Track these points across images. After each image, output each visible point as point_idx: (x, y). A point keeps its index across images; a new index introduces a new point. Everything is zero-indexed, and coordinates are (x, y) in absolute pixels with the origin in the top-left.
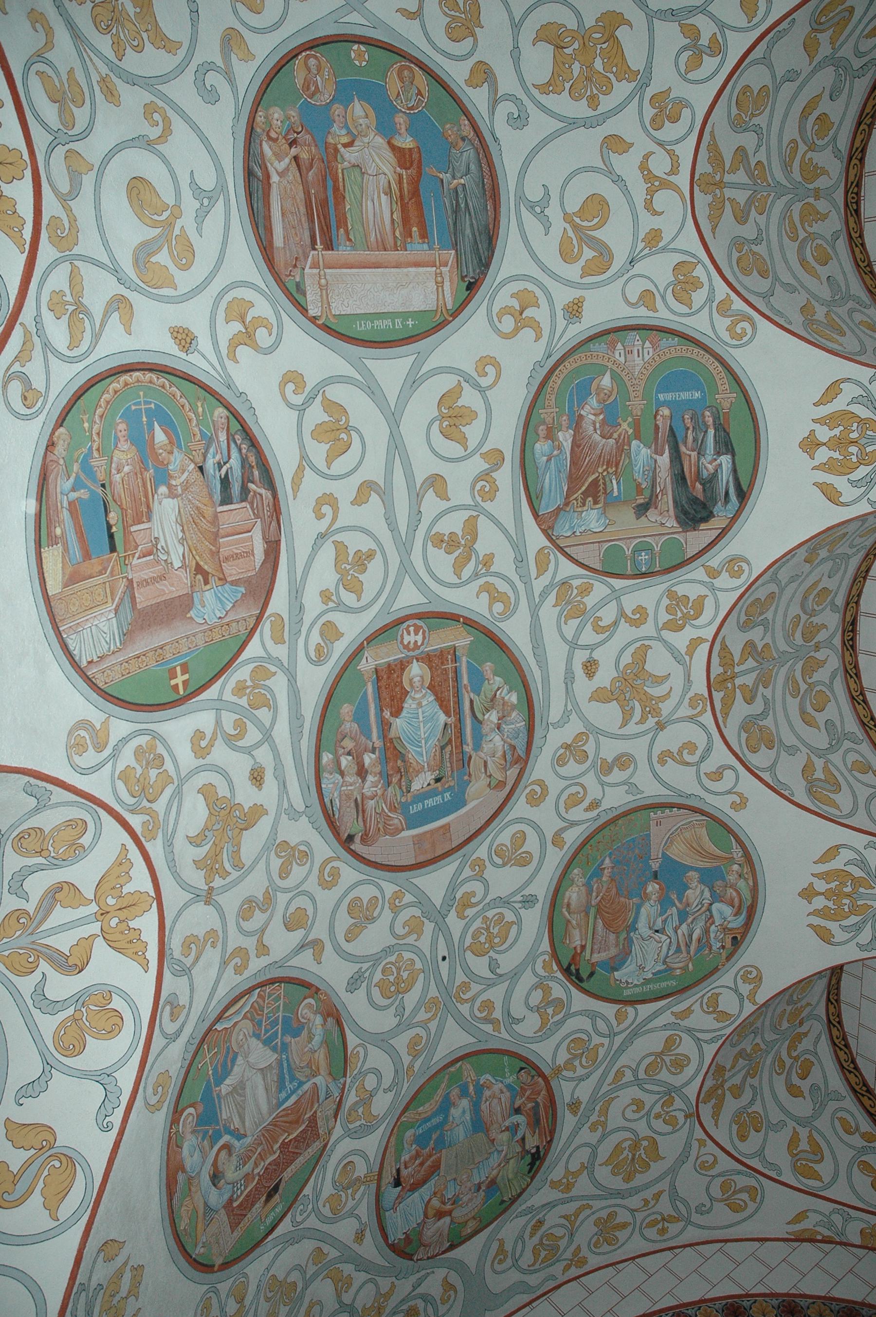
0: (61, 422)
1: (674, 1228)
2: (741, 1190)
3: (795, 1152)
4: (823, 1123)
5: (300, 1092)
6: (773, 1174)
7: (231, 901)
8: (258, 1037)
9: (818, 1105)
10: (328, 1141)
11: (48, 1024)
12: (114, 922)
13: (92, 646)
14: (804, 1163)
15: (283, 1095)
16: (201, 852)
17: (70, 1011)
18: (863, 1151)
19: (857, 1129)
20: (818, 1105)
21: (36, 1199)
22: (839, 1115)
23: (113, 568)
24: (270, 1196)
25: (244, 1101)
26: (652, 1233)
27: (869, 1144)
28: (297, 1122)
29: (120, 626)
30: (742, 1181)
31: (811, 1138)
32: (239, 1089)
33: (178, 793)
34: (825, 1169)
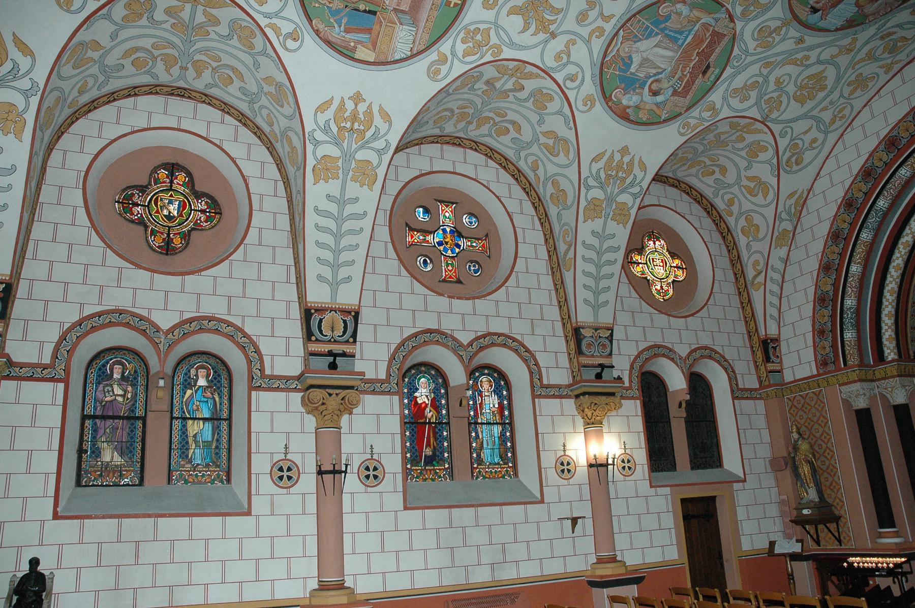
0: (310, 21)
5: (693, 32)
7: (570, 24)
8: (640, 40)
10: (736, 31)
11: (530, 104)
12: (518, 74)
13: (406, 45)
15: (680, 42)
16: (532, 29)
17: (532, 99)
21: (562, 154)
23: (382, 17)
24: (704, 73)
25: (653, 62)
28: (702, 41)
29: (408, 25)
32: (645, 62)
33: (497, 26)
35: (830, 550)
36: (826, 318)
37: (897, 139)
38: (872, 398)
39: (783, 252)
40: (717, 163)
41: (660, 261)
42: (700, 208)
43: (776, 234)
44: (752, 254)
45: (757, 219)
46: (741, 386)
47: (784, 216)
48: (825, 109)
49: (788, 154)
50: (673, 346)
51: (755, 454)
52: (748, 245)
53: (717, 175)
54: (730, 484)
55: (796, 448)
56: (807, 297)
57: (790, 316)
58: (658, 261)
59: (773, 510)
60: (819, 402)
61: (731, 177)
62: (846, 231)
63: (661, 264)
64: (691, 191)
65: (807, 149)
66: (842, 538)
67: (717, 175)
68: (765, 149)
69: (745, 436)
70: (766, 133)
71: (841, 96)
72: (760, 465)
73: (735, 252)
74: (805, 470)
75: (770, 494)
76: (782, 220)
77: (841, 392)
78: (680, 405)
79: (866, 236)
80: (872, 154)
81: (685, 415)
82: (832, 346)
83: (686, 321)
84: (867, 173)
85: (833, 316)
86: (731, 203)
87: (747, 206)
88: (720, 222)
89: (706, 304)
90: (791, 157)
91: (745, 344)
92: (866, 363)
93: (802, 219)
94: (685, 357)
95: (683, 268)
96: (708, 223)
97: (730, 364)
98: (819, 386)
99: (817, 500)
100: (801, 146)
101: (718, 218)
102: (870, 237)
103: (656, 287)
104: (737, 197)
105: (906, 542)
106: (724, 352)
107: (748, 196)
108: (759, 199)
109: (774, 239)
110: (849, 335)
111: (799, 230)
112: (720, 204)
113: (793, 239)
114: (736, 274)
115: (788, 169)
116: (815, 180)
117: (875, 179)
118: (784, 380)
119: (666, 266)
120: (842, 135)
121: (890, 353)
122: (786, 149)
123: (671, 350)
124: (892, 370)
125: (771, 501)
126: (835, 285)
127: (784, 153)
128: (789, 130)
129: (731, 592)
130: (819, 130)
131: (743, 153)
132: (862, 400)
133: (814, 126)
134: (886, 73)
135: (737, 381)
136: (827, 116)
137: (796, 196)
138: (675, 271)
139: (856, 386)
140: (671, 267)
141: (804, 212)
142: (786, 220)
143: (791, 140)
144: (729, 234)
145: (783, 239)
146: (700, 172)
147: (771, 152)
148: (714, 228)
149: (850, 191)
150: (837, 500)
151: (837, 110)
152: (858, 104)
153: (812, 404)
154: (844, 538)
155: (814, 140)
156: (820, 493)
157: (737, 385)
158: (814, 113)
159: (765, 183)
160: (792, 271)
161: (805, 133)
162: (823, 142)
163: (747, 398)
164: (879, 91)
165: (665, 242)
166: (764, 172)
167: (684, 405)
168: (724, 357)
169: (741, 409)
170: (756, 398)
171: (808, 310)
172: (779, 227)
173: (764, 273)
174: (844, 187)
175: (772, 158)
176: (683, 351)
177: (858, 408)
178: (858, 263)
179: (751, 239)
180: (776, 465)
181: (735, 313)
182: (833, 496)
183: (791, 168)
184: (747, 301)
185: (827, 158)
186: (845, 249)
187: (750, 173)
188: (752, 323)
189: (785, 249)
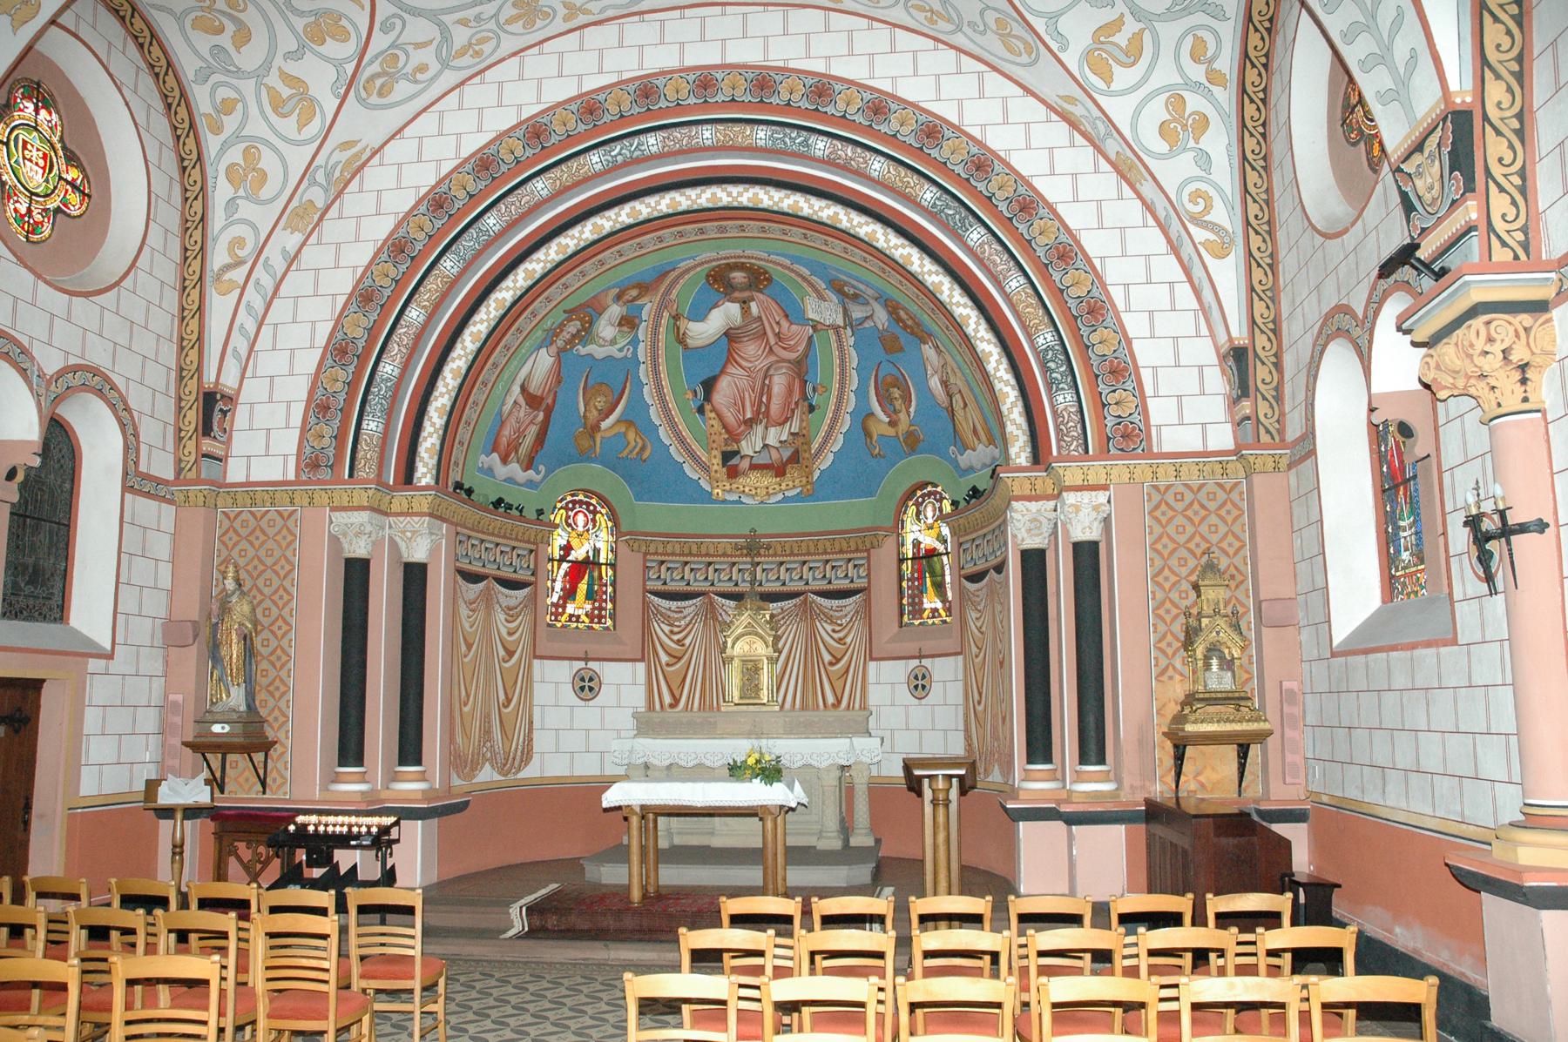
1: (943, 25)
2: (1017, 37)
3: (1102, 39)
4: (1169, 32)
6: (1054, 46)
9: (1177, 8)
14: (1104, 55)
18: (1196, 87)
19: (1210, 61)
20: (1177, 8)
22: (1200, 33)
26: (921, 16)
27: (1207, 84)
30: (1018, 30)
31: (1137, 39)
34: (1123, 77)
35: (242, 800)
36: (339, 385)
37: (545, 130)
38: (377, 544)
39: (292, 241)
40: (236, 14)
41: (41, 154)
42: (154, 87)
43: (294, 203)
44: (232, 224)
45: (268, 161)
46: (143, 468)
47: (320, 177)
48: (464, 23)
49: (376, 68)
50: (31, 344)
51: (140, 608)
52: (231, 204)
53: (225, 40)
54: (80, 659)
55: (225, 609)
56: (313, 339)
57: (267, 362)
58: (35, 153)
59: (149, 721)
60: (285, 532)
61: (249, 58)
62: (419, 247)
63: (41, 163)
64: (151, 44)
65: (406, 77)
66: (269, 781)
67: (225, 40)
68: (343, 36)
69: (130, 568)
70: (363, 8)
71: (496, 15)
72: (143, 631)
73: (198, 205)
74: (233, 651)
75: (150, 688)
76: (314, 182)
77: (331, 522)
78: (11, 475)
79: (449, 265)
80: (501, 136)
81: (15, 498)
82: (335, 437)
83: (70, 302)
84: (483, 163)
85: (352, 385)
86: (227, 107)
87: (257, 128)
88: (188, 136)
89: (117, 284)
90: (378, 75)
91: (167, 389)
92: (384, 479)
93: (346, 197)
94: (52, 377)
95: (82, 192)
96: (161, 125)
97: (132, 417)
98: (292, 503)
99: (243, 708)
100: (400, 65)
101: (186, 125)
102: (455, 271)
103: (17, 205)
104: (245, 107)
105: (372, 791)
106: (127, 391)
107: (268, 110)
108: (289, 126)
109: (288, 211)
110: (373, 425)
111: (333, 212)
112: (202, 98)
113: (317, 224)
114: (186, 250)
115: (364, 94)
116: (392, 137)
117: (494, 179)
118: (225, 477)
119: (50, 171)
120: (463, 83)
121: (424, 473)
122: (376, 57)
123: (24, 351)
124: (423, 502)
125: (149, 701)
126: (372, 332)
127: (371, 62)
128: (398, 23)
129: (34, 881)
130: (438, 56)
131: (299, 23)
132: (362, 544)
133: (435, 43)
134: (565, 19)
135: (138, 456)
136: (461, 36)
137: (354, 150)
138: (67, 191)
139: (364, 516)
140: (61, 178)
141: (354, 185)
142: (320, 185)
143: (393, 45)
144: (198, 166)
145: (302, 218)
146: (193, 16)
147: (350, 48)
148: (170, 142)
149: (447, 181)
150: (276, 711)
151: (479, 36)
152: (509, 45)
153: (271, 532)
154: (274, 780)
155: (422, 68)
156: (250, 696)
157: (136, 463)
158: (448, 19)
159: (312, 100)
160: (296, 283)
161: (418, 46)
162: (433, 79)
163: (148, 495)
164: (541, 42)
165: (61, 119)
166: (321, 80)
167: (20, 477)
168: (125, 402)
169: (133, 514)
170: (163, 499)
171: (309, 361)
172: (305, 191)
173: (246, 268)
174: (438, 169)
175: (347, 60)
176: (51, 362)
177: (352, 555)
178: (424, 307)
179: (241, 192)
180: (173, 634)
181: (164, 322)
182: (271, 703)
183: (369, 95)
184: (195, 307)
185: (425, 110)
186: (407, 275)
187: (292, 68)
188: (193, 355)
189: (298, 238)
